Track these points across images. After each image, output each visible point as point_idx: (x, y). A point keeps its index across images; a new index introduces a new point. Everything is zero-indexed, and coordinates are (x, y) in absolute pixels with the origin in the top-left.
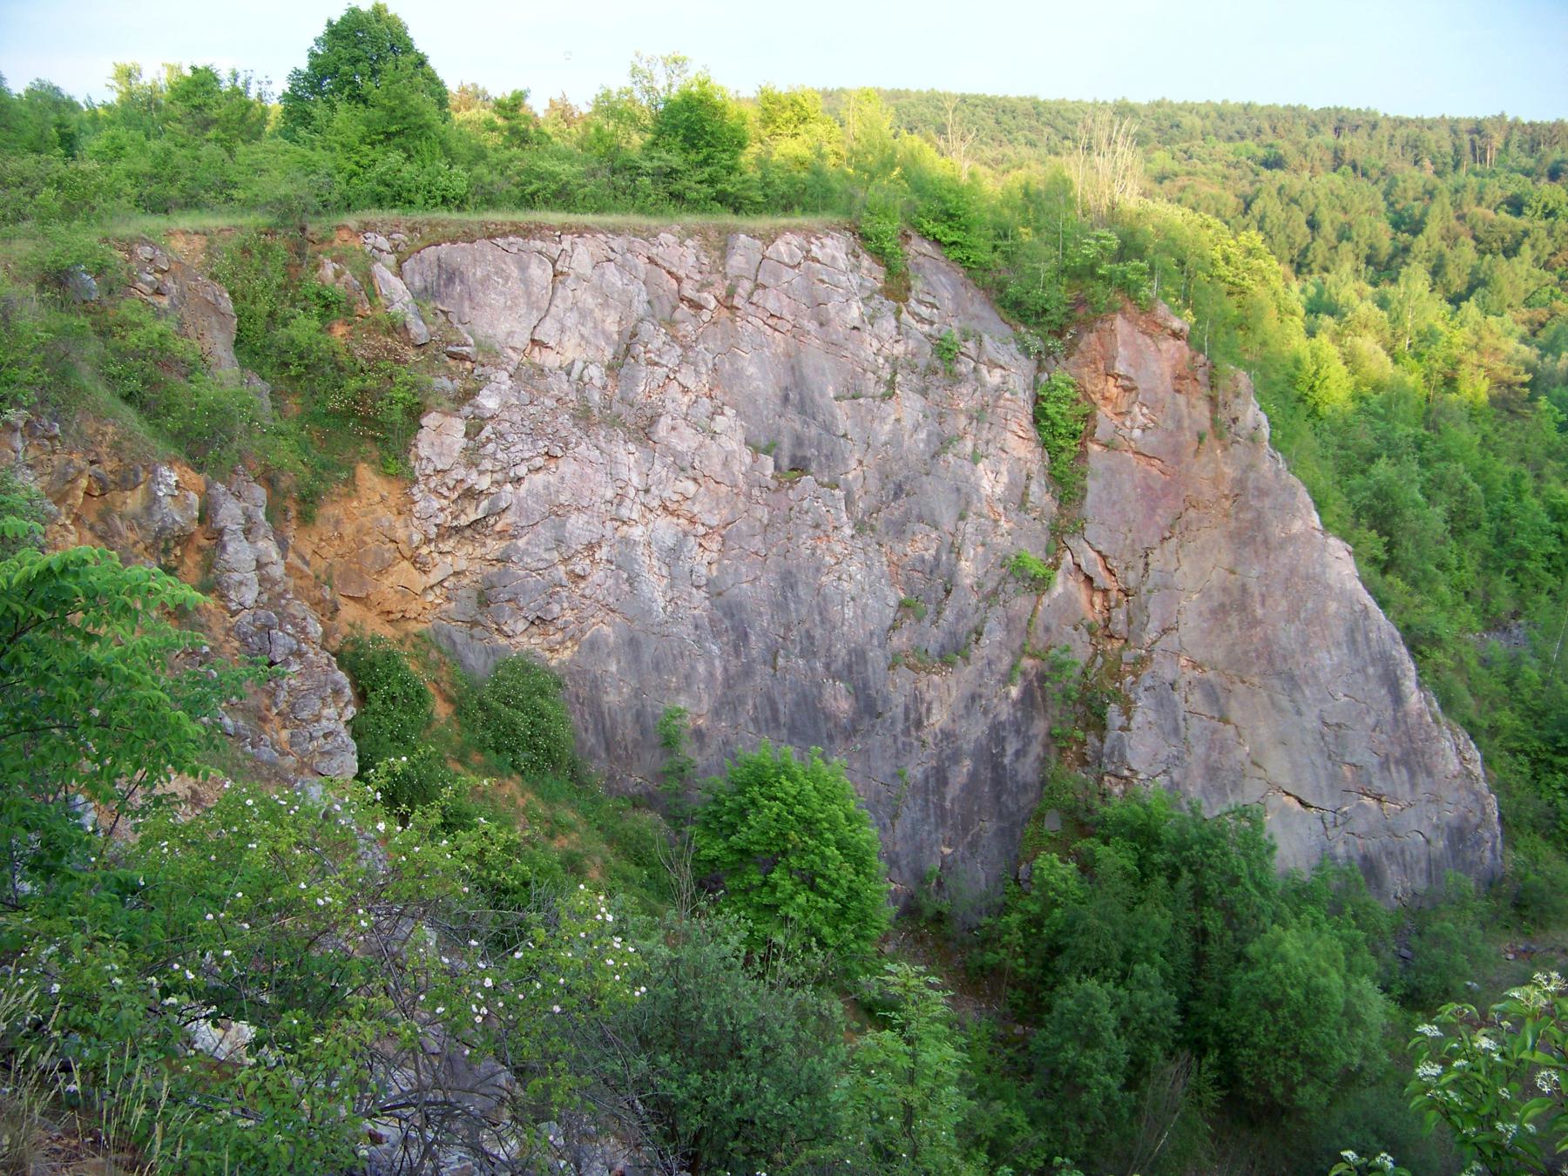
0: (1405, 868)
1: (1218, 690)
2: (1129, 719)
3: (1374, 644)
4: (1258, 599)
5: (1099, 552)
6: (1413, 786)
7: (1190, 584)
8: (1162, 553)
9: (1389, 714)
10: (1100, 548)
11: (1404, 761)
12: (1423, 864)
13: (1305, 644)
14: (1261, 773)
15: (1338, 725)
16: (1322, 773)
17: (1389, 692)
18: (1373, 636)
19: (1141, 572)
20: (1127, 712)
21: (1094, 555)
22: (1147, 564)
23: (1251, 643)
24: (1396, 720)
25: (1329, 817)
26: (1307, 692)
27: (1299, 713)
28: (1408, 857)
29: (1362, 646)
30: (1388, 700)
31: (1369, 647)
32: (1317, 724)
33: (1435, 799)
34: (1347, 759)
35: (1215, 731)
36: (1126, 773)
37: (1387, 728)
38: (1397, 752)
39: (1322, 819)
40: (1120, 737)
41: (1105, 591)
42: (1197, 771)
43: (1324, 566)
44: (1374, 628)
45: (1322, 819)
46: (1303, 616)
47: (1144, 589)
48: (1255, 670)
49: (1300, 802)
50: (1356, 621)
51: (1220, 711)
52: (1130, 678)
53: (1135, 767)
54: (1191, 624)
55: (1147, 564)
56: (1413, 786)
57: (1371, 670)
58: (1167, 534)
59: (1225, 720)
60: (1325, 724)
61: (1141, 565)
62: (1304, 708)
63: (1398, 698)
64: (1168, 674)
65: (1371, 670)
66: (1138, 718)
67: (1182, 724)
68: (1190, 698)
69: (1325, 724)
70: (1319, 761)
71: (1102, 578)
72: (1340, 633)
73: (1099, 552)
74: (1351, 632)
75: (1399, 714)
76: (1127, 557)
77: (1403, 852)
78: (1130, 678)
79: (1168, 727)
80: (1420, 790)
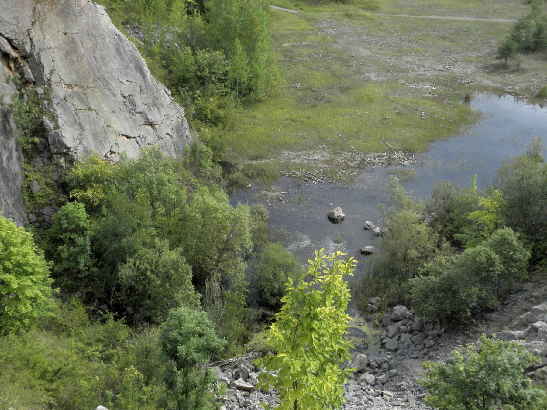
0: (168, 150)
1: (82, 95)
2: (56, 122)
3: (128, 53)
4: (80, 44)
5: (7, 39)
6: (160, 113)
7: (52, 44)
8: (35, 31)
9: (143, 85)
10: (7, 36)
11: (154, 104)
12: (173, 148)
13: (104, 60)
14: (111, 130)
15: (129, 96)
16: (129, 119)
17: (140, 74)
18: (126, 49)
19: (29, 43)
20: (54, 118)
21: (5, 41)
22: (31, 39)
23: (84, 67)
24: (146, 86)
25: (138, 139)
26: (113, 84)
27: (114, 95)
28: (168, 146)
29: (124, 55)
30: (141, 79)
31: (127, 55)
32: (122, 98)
33: (168, 117)
34: (138, 111)
35: (89, 116)
36: (65, 150)
37: (145, 91)
38: (150, 101)
39: (137, 142)
40: (56, 133)
41: (15, 60)
42: (90, 138)
43: (99, 20)
44: (126, 45)
45: (137, 142)
46: (98, 47)
47: (35, 53)
48: (90, 80)
49: (128, 137)
50: (118, 44)
51: (86, 105)
52: (46, 102)
53: (69, 146)
54: (60, 65)
55: (31, 39)
56: (160, 113)
57: (131, 65)
58: (33, 20)
59: (90, 109)
60: (124, 97)
61: (28, 40)
62: (115, 92)
63: (144, 76)
64: (61, 94)
65: (131, 65)
66: (60, 122)
67: (76, 117)
68: (75, 103)
69: (124, 97)
70: (127, 116)
71: (14, 54)
72: (114, 51)
73: (7, 39)
74: (118, 50)
75: (146, 83)
76: (22, 37)
77: (166, 145)
78: (46, 102)
79: (72, 120)
80: (163, 115)
